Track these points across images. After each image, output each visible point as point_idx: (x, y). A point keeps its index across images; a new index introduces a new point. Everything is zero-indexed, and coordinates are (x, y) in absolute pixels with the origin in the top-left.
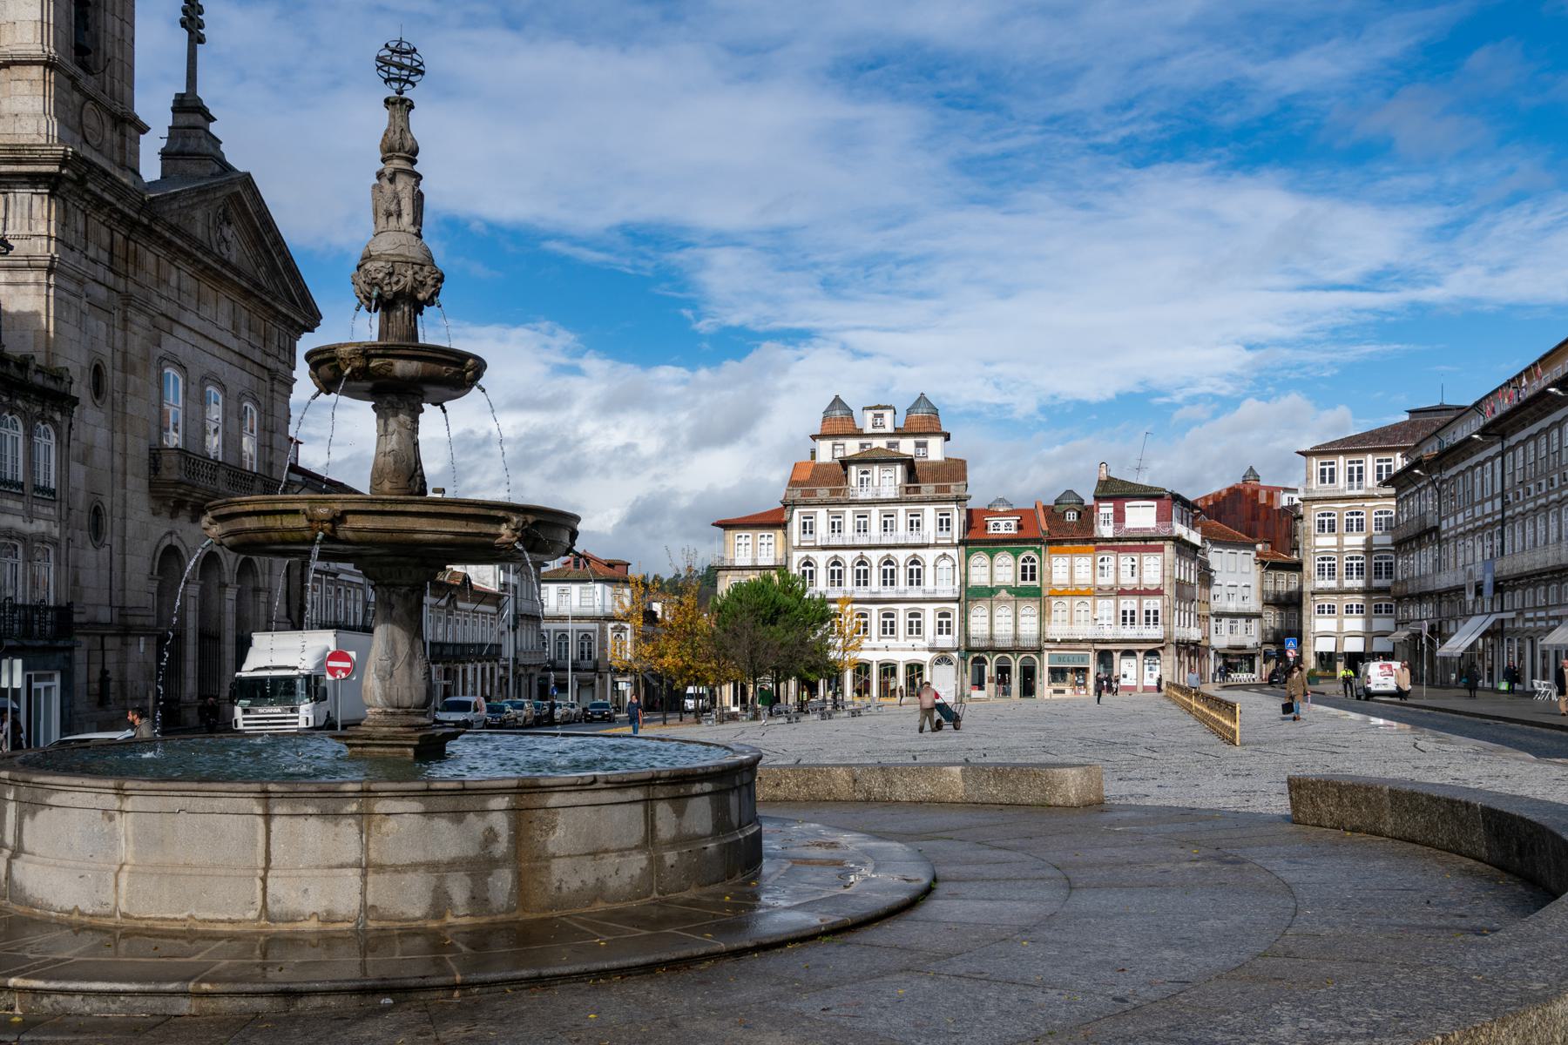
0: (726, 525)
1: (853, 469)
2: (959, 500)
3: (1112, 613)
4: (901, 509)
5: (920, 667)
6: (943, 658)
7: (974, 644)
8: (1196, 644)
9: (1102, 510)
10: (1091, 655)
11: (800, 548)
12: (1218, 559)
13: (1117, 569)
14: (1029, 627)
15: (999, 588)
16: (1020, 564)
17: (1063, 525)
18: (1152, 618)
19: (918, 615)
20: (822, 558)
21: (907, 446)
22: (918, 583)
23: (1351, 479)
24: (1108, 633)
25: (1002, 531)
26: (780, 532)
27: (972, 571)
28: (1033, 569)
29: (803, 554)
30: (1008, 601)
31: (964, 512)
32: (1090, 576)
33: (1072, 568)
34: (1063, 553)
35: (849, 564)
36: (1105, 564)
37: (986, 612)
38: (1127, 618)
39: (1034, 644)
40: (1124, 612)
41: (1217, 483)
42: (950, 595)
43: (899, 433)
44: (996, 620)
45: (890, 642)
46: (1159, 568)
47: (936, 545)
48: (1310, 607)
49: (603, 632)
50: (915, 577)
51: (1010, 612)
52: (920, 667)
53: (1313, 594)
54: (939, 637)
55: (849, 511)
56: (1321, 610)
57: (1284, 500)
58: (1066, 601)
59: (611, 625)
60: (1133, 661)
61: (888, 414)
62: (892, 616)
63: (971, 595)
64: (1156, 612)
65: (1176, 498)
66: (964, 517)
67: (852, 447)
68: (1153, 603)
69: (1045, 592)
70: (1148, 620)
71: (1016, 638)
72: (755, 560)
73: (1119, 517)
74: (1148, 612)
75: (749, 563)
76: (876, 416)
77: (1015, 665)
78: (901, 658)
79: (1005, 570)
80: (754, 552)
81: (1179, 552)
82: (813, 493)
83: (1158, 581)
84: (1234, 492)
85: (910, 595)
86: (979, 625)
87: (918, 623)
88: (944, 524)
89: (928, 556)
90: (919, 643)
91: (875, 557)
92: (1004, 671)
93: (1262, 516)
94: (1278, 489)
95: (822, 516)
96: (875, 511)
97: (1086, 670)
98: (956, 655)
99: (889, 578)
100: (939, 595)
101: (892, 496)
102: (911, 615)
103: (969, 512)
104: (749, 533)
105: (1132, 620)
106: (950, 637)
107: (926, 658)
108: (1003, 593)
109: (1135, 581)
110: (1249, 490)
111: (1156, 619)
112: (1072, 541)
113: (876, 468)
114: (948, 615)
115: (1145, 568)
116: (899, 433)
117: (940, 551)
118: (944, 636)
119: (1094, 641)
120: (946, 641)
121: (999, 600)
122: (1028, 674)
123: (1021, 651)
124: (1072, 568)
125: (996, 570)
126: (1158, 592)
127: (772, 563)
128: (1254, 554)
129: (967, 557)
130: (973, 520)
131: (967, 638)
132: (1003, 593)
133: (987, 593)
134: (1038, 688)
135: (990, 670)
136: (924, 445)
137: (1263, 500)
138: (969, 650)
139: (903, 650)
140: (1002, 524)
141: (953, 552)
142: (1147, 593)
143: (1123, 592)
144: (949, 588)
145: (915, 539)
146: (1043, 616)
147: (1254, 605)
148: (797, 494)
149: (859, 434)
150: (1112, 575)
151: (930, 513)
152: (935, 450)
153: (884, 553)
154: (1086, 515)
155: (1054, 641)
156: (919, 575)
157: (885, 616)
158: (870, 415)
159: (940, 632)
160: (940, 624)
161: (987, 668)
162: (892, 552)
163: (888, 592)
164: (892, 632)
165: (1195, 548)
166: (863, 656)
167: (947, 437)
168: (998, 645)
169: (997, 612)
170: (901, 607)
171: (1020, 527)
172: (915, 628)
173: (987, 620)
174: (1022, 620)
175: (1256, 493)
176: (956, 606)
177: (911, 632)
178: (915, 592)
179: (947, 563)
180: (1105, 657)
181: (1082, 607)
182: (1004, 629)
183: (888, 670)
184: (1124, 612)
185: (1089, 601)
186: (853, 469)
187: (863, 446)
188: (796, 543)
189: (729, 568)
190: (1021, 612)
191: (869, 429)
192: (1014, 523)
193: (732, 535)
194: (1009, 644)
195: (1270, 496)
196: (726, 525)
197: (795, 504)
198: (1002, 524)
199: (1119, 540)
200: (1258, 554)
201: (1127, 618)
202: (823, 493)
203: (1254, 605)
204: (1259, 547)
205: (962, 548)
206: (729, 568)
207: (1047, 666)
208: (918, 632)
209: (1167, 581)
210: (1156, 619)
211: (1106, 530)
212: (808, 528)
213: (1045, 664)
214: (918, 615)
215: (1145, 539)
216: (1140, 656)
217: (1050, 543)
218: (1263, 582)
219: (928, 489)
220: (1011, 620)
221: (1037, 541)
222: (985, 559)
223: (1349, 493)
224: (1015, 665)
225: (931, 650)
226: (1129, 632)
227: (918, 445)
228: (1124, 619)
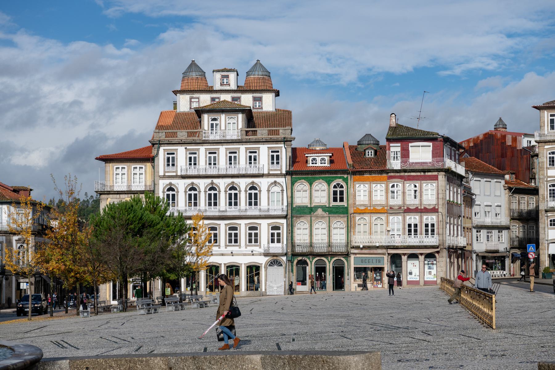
0: (107, 159)
1: (206, 117)
2: (285, 141)
3: (401, 226)
4: (242, 148)
5: (258, 268)
6: (275, 261)
7: (298, 250)
8: (462, 249)
9: (392, 149)
10: (386, 257)
11: (164, 177)
12: (477, 185)
13: (404, 193)
14: (339, 237)
15: (317, 207)
16: (332, 189)
17: (365, 161)
18: (430, 229)
19: (256, 229)
20: (181, 185)
21: (247, 100)
22: (256, 204)
24: (398, 241)
25: (319, 164)
26: (149, 165)
27: (297, 194)
28: (342, 193)
29: (167, 181)
30: (323, 217)
31: (290, 150)
32: (384, 198)
33: (370, 192)
34: (364, 181)
35: (202, 189)
36: (395, 189)
37: (307, 226)
38: (412, 229)
39: (343, 250)
40: (410, 225)
42: (280, 213)
43: (241, 90)
44: (315, 232)
45: (235, 249)
46: (435, 192)
47: (269, 175)
48: (544, 221)
49: (9, 243)
50: (253, 199)
51: (325, 226)
52: (258, 268)
53: (546, 211)
54: (272, 245)
55: (202, 149)
57: (524, 143)
58: (367, 217)
59: (15, 238)
60: (416, 262)
61: (232, 76)
62: (235, 229)
63: (295, 213)
64: (433, 225)
65: (446, 140)
66: (290, 154)
67: (205, 100)
68: (430, 219)
69: (351, 210)
70: (427, 231)
71: (330, 245)
72: (129, 186)
73: (405, 154)
75: (125, 189)
76: (223, 77)
77: (329, 266)
78: (243, 261)
79: (320, 193)
80: (129, 180)
81: (449, 181)
82: (175, 135)
83: (434, 202)
84: (488, 136)
85: (249, 213)
86: (301, 236)
87: (256, 235)
88: (275, 159)
89: (264, 183)
90: (257, 249)
91: (222, 183)
92: (321, 270)
93: (509, 154)
94: (520, 135)
95: (181, 153)
96: (222, 150)
97: (381, 269)
98: (284, 258)
99: (233, 200)
100: (272, 213)
101: (235, 137)
102: (251, 228)
103: (294, 150)
104: (125, 165)
105: (416, 231)
106: (280, 245)
107: (262, 261)
108: (320, 211)
109: (417, 202)
110: (499, 135)
111: (433, 231)
112: (370, 172)
113: (223, 116)
114: (277, 228)
115: (424, 193)
116: (241, 90)
117: (272, 180)
118: (276, 245)
119: (388, 247)
120: (277, 248)
121: (317, 217)
122: (339, 272)
123: (333, 255)
124: (370, 192)
125: (315, 194)
126: (434, 210)
127: (143, 189)
128: (503, 182)
129: (293, 184)
130: (296, 156)
131: (293, 246)
132: (320, 211)
133: (308, 211)
134: (346, 283)
135: (310, 270)
136: (260, 99)
137: (509, 142)
138: (295, 255)
139: (245, 255)
140: (319, 159)
141: (281, 180)
142: (426, 211)
143: (408, 211)
144: (279, 207)
145: (253, 170)
146: (350, 229)
147: (504, 220)
148: (162, 136)
149: (210, 90)
150: (400, 198)
151: (264, 151)
152: (268, 103)
153: (229, 180)
154: (381, 153)
155: (358, 248)
156: (256, 198)
157: (230, 229)
158: (218, 76)
159: (273, 241)
160: (273, 235)
161: (308, 269)
162: (236, 180)
163: (233, 211)
164: (236, 241)
165: (461, 177)
166: (213, 260)
167: (277, 94)
168: (317, 250)
169: (315, 226)
170: (243, 222)
171: (331, 162)
172: (254, 238)
173: (307, 232)
174: (334, 232)
175: (504, 137)
176: (284, 221)
177: (250, 241)
178: (253, 211)
179: (277, 189)
180: (396, 260)
181: (378, 222)
182: (320, 238)
183: (234, 270)
184: (410, 225)
185: (383, 217)
186: (206, 117)
187: (213, 99)
188: (161, 173)
189: (109, 193)
190: (333, 226)
191: (217, 87)
192: (327, 159)
193: (112, 167)
194: (324, 250)
195: (514, 140)
196: (107, 159)
197: (160, 143)
198: (319, 159)
199: (405, 171)
200: (506, 182)
201: (412, 229)
202: (182, 135)
203: (504, 220)
204: (507, 177)
205: (288, 177)
206: (109, 193)
207: (353, 266)
208: (256, 241)
209: (441, 202)
210: (433, 231)
211: (395, 164)
212: (171, 161)
213: (351, 265)
214: (256, 229)
215: (424, 171)
216: (422, 258)
217: (354, 173)
218: (510, 203)
219: (262, 133)
220: (325, 231)
221: (345, 172)
222: (306, 186)
224: (329, 266)
225: (266, 255)
226: (413, 240)
227: (255, 99)
228: (410, 231)
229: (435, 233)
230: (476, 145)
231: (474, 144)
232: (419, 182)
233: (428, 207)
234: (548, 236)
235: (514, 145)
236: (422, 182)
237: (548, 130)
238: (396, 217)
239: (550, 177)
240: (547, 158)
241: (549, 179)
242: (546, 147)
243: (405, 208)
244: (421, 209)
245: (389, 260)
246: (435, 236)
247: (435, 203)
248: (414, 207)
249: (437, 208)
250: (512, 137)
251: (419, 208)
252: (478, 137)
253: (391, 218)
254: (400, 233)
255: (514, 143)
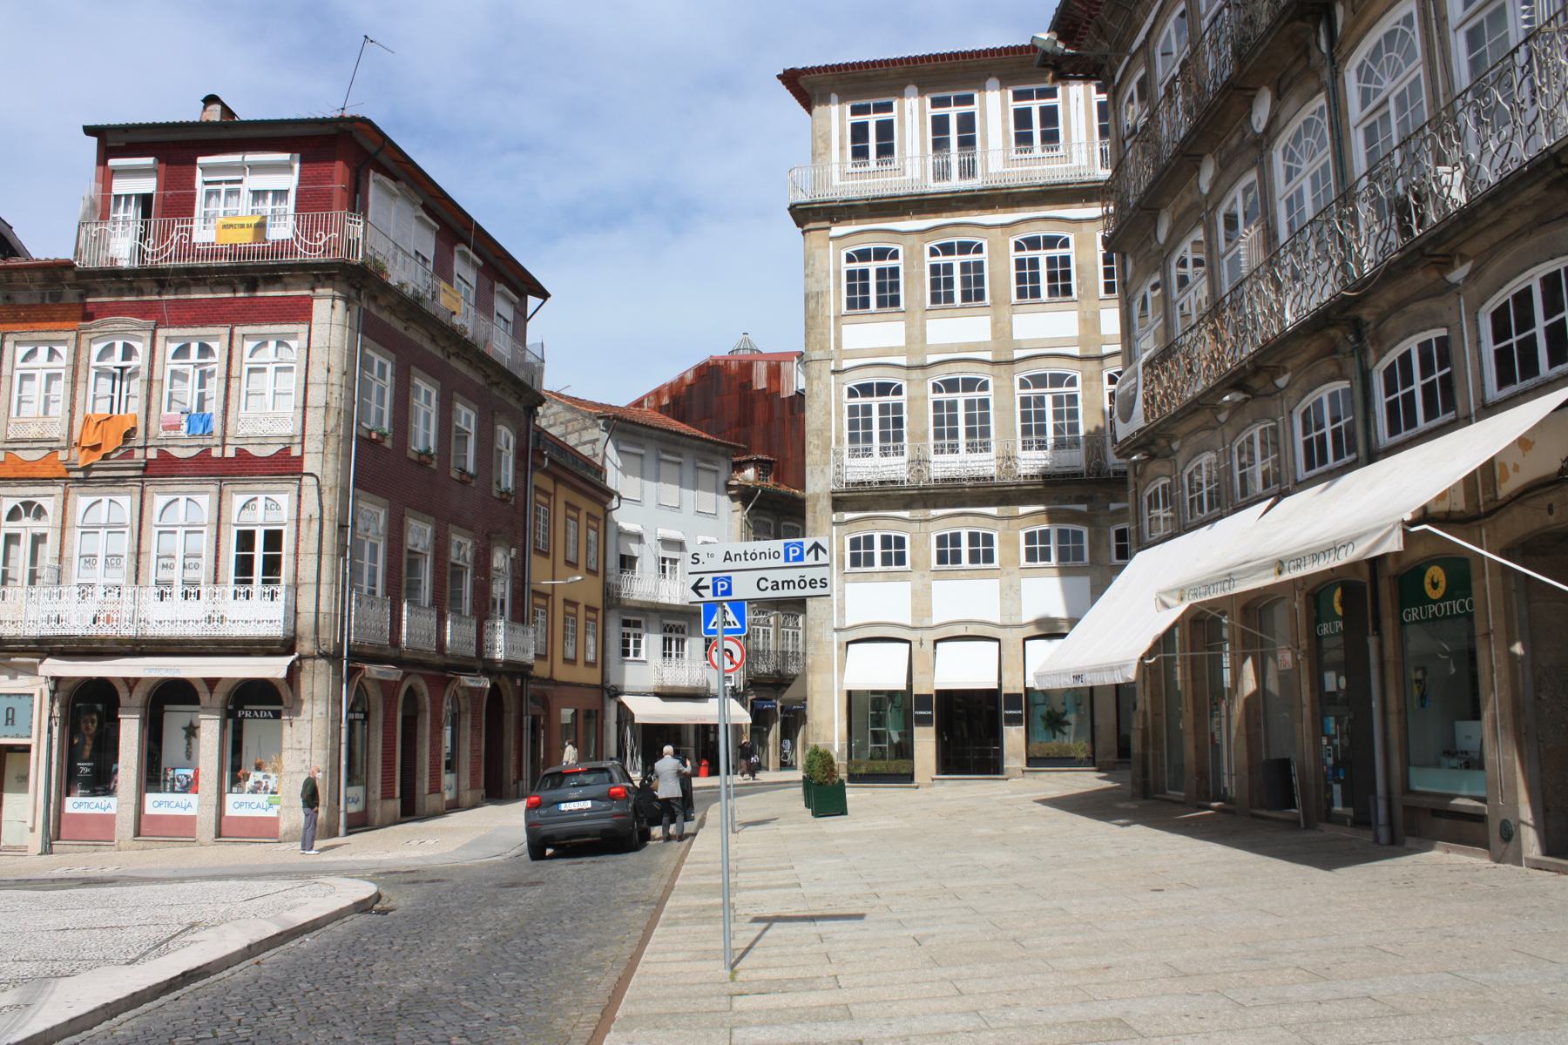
18: (257, 558)
23: (940, 144)
41: (674, 367)
56: (860, 555)
64: (273, 539)
68: (265, 507)
70: (244, 567)
74: (246, 539)
81: (368, 329)
83: (290, 428)
84: (709, 373)
93: (760, 410)
94: (788, 356)
111: (272, 566)
126: (284, 466)
137: (760, 382)
195: (775, 372)
223: (934, 186)
229: (283, 578)
230: (675, 399)
231: (672, 398)
232: (223, 331)
233: (255, 451)
234: (842, 610)
235: (774, 389)
236: (238, 330)
237: (842, 162)
238: (105, 500)
239: (853, 354)
240: (838, 273)
241: (846, 364)
242: (837, 230)
243: (152, 454)
244: (223, 459)
245: (56, 712)
246: (281, 590)
247: (289, 431)
248: (193, 452)
249: (296, 451)
250: (769, 367)
251: (216, 453)
252: (682, 379)
253: (81, 501)
254: (122, 575)
255: (774, 382)
